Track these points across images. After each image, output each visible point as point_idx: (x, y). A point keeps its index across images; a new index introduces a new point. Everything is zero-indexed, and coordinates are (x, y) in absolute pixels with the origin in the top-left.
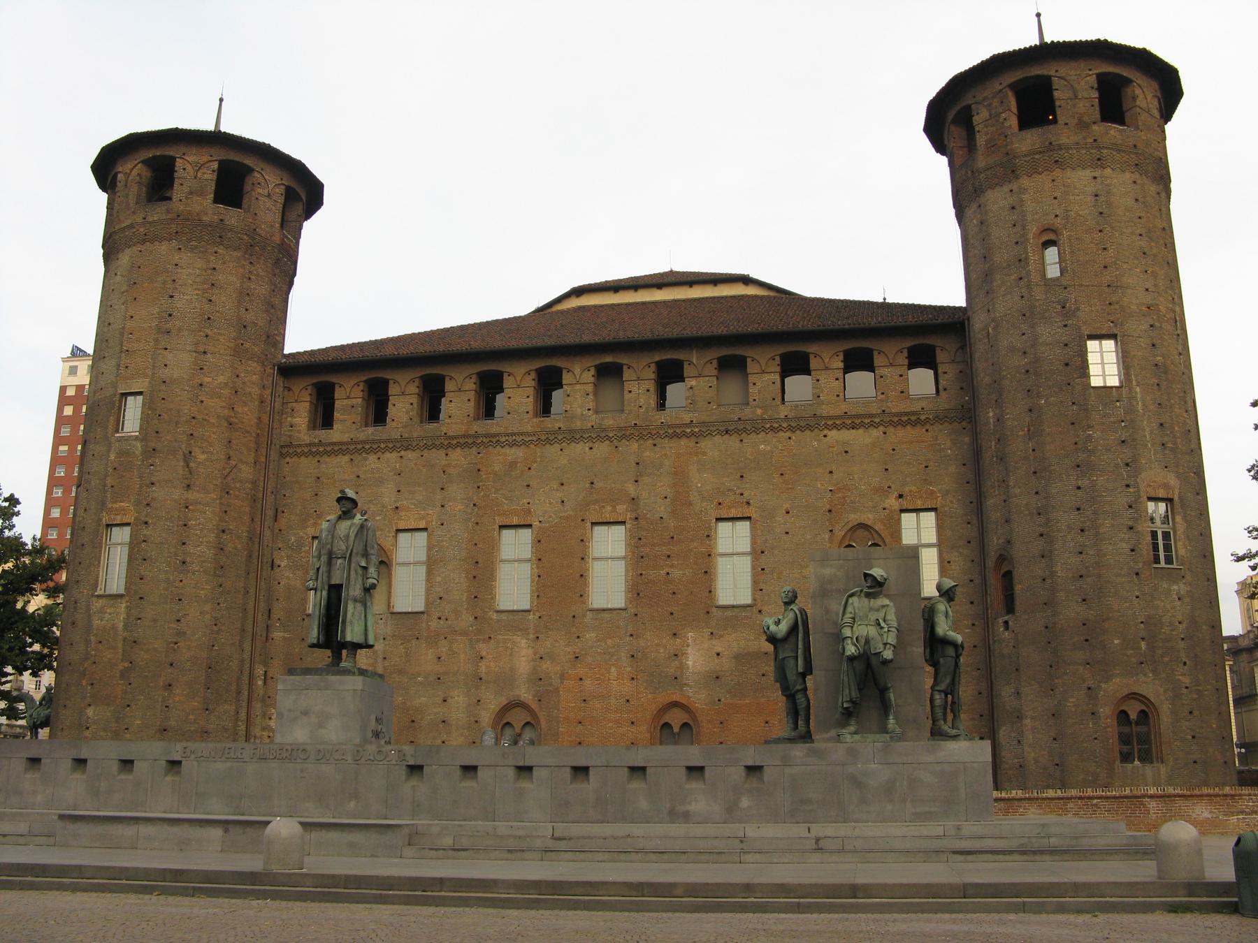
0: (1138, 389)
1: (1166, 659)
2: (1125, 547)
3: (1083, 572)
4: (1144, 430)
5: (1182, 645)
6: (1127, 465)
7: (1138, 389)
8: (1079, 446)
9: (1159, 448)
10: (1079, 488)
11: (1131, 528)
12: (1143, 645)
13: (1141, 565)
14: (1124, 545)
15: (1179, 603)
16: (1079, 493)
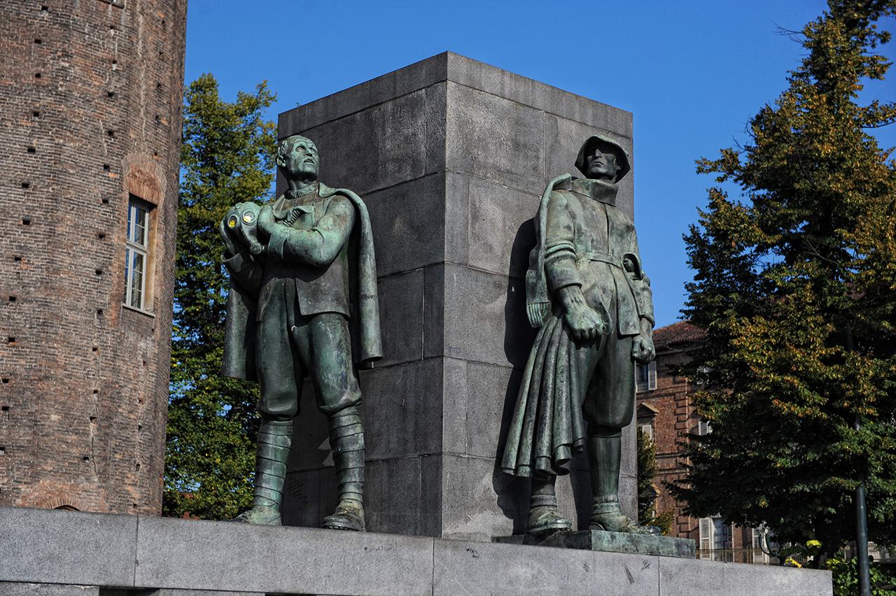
0: (141, 19)
1: (118, 456)
2: (89, 264)
3: (17, 292)
4: (140, 87)
5: (138, 437)
6: (111, 133)
7: (141, 19)
8: (45, 80)
9: (152, 122)
10: (32, 150)
11: (101, 236)
12: (92, 427)
13: (107, 298)
14: (88, 261)
15: (142, 370)
16: (32, 159)
